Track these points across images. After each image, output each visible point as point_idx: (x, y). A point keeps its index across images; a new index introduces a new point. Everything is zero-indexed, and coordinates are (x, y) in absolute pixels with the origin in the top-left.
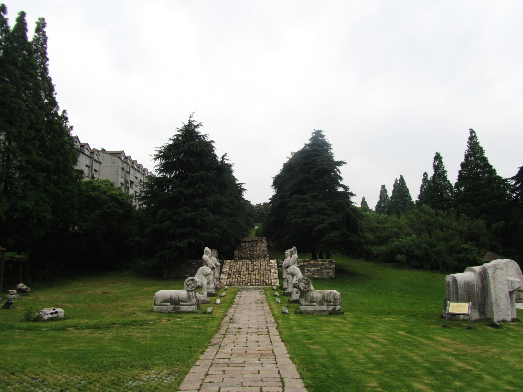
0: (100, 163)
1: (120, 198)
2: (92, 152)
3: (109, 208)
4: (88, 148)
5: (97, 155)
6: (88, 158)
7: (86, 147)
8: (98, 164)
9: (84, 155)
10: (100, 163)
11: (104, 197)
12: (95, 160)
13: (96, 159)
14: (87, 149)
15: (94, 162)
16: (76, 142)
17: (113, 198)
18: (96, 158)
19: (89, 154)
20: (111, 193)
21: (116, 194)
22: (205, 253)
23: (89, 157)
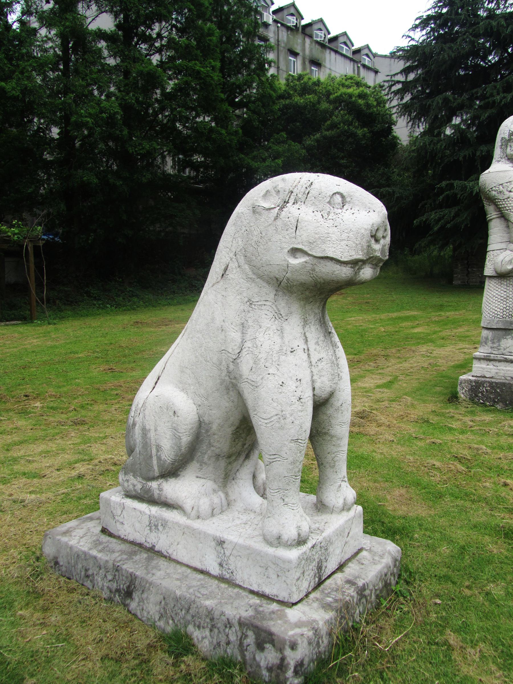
0: (376, 72)
1: (361, 102)
2: (357, 52)
3: (334, 126)
4: (348, 43)
5: (367, 55)
6: (348, 62)
7: (342, 39)
8: (372, 74)
9: (338, 57)
10: (376, 72)
11: (324, 106)
12: (364, 66)
13: (367, 64)
14: (345, 43)
15: (361, 69)
16: (320, 30)
17: (347, 103)
18: (367, 61)
19: (351, 56)
20: (339, 94)
21: (350, 96)
22: (497, 152)
23: (351, 60)
